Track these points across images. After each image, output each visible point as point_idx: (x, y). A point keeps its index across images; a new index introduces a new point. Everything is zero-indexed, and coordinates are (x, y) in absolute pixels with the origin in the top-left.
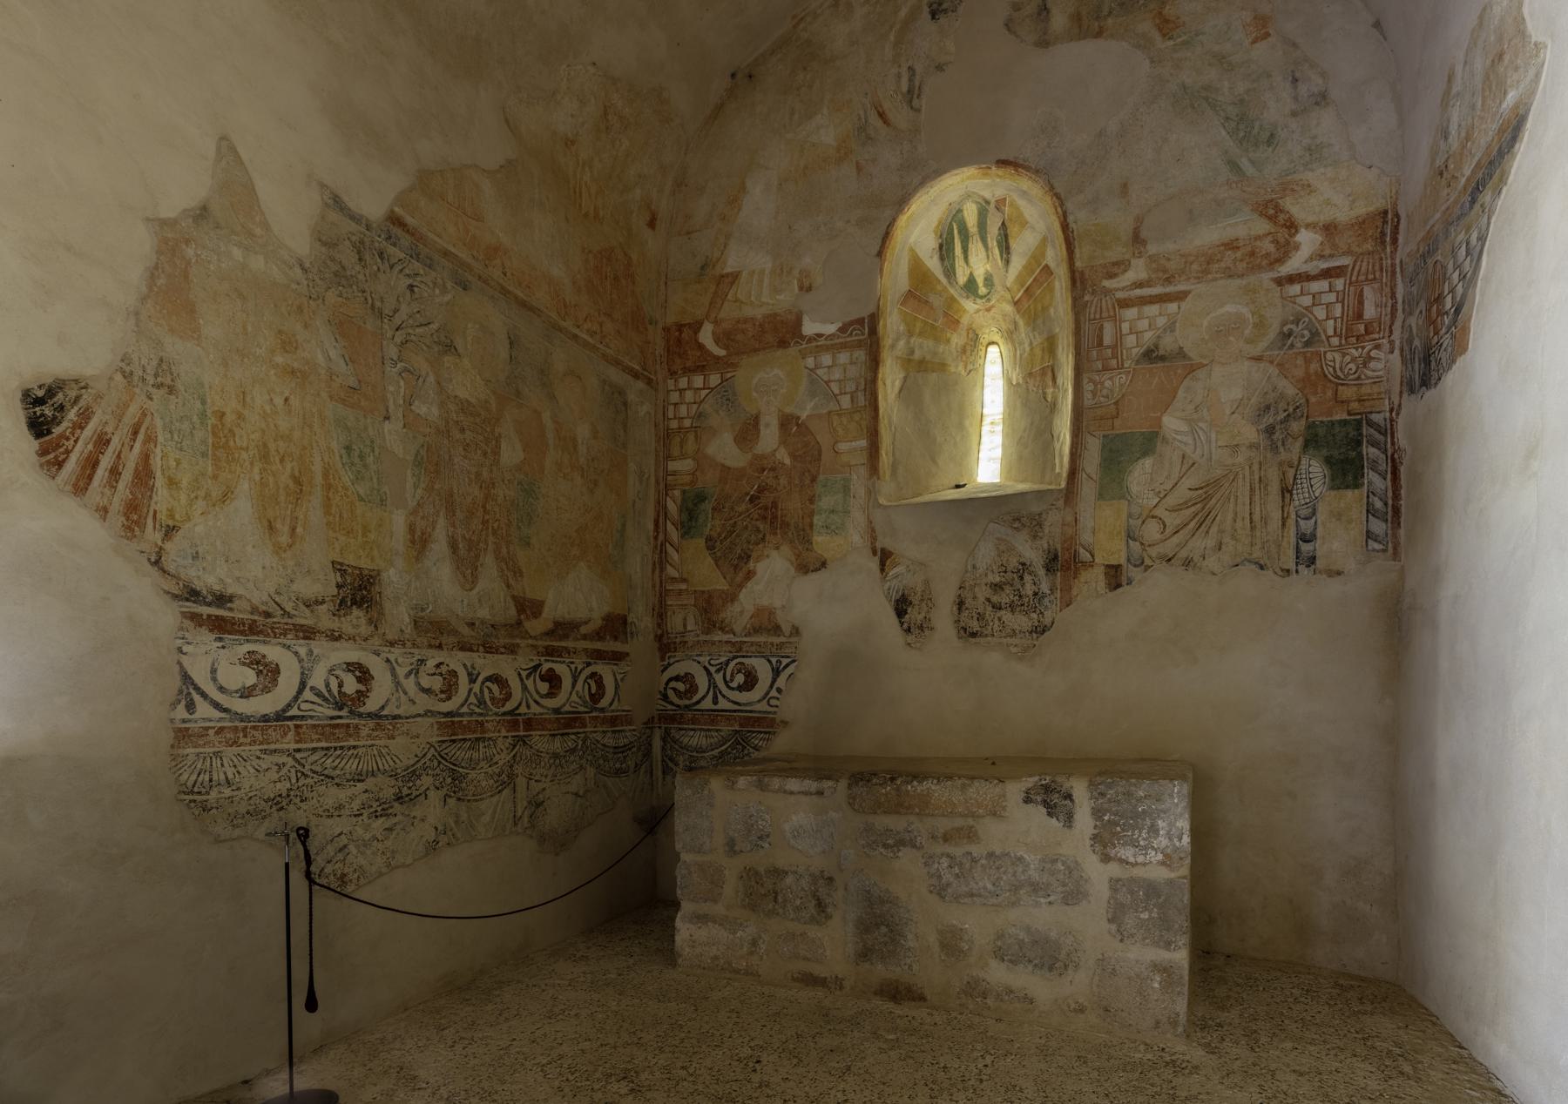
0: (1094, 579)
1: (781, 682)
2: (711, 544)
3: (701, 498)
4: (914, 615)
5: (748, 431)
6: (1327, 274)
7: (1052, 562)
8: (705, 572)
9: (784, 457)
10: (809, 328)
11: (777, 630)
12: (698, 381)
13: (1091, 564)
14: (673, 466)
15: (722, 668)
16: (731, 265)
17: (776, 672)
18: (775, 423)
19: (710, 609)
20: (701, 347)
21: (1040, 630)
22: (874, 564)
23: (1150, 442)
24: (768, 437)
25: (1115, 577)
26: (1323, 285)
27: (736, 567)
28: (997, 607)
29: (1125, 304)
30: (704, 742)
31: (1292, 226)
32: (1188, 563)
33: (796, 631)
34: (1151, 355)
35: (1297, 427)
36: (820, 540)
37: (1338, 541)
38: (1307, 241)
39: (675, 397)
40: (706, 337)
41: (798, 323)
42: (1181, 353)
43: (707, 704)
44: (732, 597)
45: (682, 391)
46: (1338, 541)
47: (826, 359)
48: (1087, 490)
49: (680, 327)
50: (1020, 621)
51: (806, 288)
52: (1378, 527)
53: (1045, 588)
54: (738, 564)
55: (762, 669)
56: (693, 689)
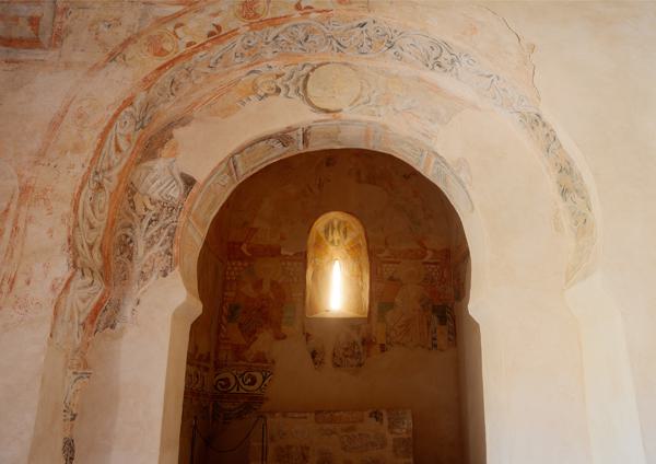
0: (377, 348)
1: (266, 382)
2: (240, 325)
3: (237, 308)
4: (318, 359)
5: (258, 284)
6: (436, 264)
7: (364, 342)
8: (237, 337)
9: (271, 295)
10: (283, 252)
11: (266, 361)
12: (240, 264)
13: (375, 343)
14: (226, 294)
15: (242, 375)
16: (255, 225)
17: (265, 378)
18: (269, 285)
19: (238, 351)
20: (241, 251)
21: (360, 365)
22: (304, 338)
23: (392, 305)
24: (266, 288)
25: (383, 348)
26: (433, 266)
27: (250, 336)
28: (346, 356)
29: (384, 262)
30: (232, 407)
31: (425, 248)
32: (403, 345)
33: (273, 362)
34: (391, 279)
35: (430, 306)
36: (285, 329)
37: (442, 341)
38: (430, 253)
39: (229, 268)
40: (244, 248)
41: (279, 251)
42: (399, 280)
43: (235, 390)
44: (248, 348)
45: (233, 267)
46: (442, 341)
47: (289, 264)
48: (374, 319)
49: (234, 243)
50: (354, 362)
51: (282, 238)
52: (452, 337)
53: (361, 350)
54: (251, 335)
55: (259, 377)
56: (229, 384)
